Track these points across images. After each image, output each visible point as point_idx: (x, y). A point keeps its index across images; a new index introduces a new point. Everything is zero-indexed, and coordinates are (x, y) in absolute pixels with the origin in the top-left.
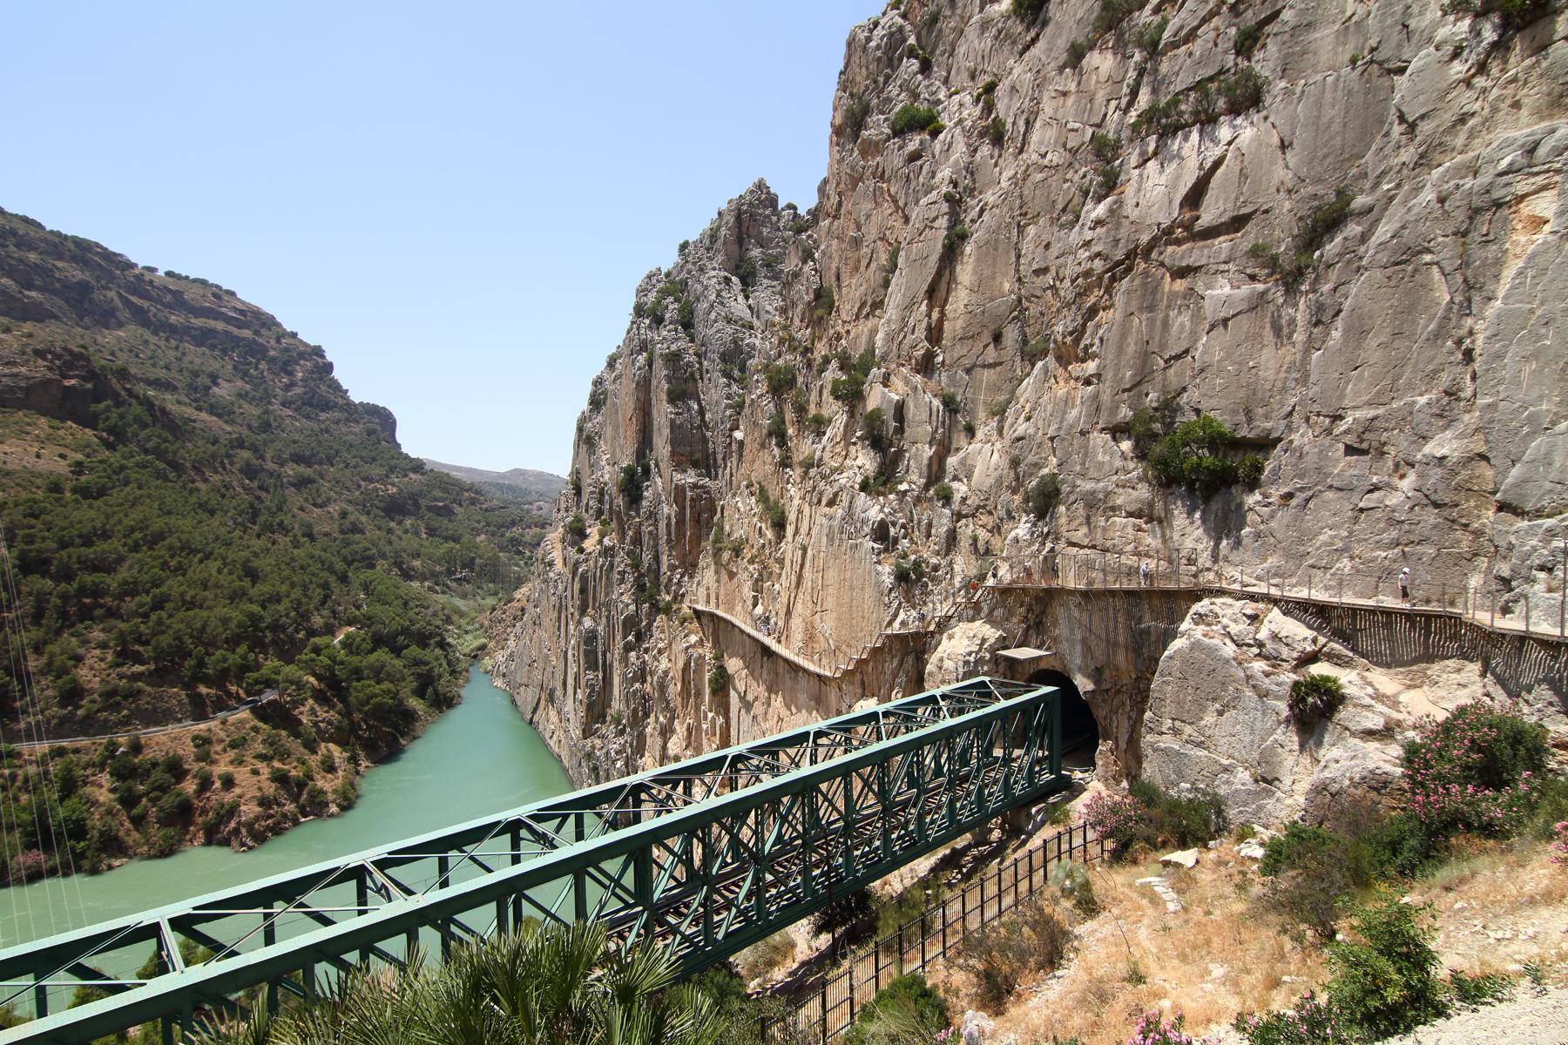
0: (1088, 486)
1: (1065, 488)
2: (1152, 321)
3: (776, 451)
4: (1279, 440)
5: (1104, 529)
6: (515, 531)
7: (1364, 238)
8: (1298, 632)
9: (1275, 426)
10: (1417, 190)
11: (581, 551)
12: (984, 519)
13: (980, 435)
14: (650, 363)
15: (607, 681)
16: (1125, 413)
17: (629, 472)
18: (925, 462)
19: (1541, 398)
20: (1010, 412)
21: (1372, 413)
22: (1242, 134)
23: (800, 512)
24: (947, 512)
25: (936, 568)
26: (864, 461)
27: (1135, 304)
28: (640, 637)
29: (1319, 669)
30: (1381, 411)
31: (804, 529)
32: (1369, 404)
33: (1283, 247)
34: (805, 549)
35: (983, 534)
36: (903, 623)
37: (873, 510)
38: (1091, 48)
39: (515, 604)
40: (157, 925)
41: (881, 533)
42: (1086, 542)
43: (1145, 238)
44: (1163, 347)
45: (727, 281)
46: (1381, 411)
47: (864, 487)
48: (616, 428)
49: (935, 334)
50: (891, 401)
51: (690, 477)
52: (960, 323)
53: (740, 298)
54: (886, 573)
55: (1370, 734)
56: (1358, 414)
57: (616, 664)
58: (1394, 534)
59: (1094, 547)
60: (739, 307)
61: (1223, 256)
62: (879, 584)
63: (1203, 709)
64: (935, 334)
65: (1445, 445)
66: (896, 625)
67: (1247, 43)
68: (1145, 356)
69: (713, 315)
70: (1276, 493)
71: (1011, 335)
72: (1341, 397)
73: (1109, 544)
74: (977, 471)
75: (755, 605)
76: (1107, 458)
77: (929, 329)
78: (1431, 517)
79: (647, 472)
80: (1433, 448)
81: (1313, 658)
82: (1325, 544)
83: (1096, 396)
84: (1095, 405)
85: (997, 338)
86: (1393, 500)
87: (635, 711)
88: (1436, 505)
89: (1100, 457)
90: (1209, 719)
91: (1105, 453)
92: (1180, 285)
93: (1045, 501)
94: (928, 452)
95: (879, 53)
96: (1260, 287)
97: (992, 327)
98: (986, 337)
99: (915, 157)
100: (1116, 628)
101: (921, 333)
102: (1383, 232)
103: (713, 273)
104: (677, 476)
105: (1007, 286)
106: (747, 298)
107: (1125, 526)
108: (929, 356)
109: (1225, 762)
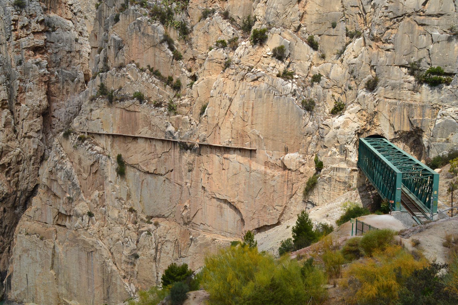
5: (399, 94)
12: (337, 90)
13: (327, 59)
16: (405, 62)
42: (392, 97)
47: (278, 76)
49: (302, 17)
59: (395, 99)
61: (436, 24)
64: (302, 17)
71: (341, 27)
73: (401, 98)
76: (399, 74)
85: (334, 26)
90: (450, 136)
91: (397, 72)
96: (449, 35)
97: (331, 21)
100: (404, 121)
107: (408, 93)
109: (455, 144)
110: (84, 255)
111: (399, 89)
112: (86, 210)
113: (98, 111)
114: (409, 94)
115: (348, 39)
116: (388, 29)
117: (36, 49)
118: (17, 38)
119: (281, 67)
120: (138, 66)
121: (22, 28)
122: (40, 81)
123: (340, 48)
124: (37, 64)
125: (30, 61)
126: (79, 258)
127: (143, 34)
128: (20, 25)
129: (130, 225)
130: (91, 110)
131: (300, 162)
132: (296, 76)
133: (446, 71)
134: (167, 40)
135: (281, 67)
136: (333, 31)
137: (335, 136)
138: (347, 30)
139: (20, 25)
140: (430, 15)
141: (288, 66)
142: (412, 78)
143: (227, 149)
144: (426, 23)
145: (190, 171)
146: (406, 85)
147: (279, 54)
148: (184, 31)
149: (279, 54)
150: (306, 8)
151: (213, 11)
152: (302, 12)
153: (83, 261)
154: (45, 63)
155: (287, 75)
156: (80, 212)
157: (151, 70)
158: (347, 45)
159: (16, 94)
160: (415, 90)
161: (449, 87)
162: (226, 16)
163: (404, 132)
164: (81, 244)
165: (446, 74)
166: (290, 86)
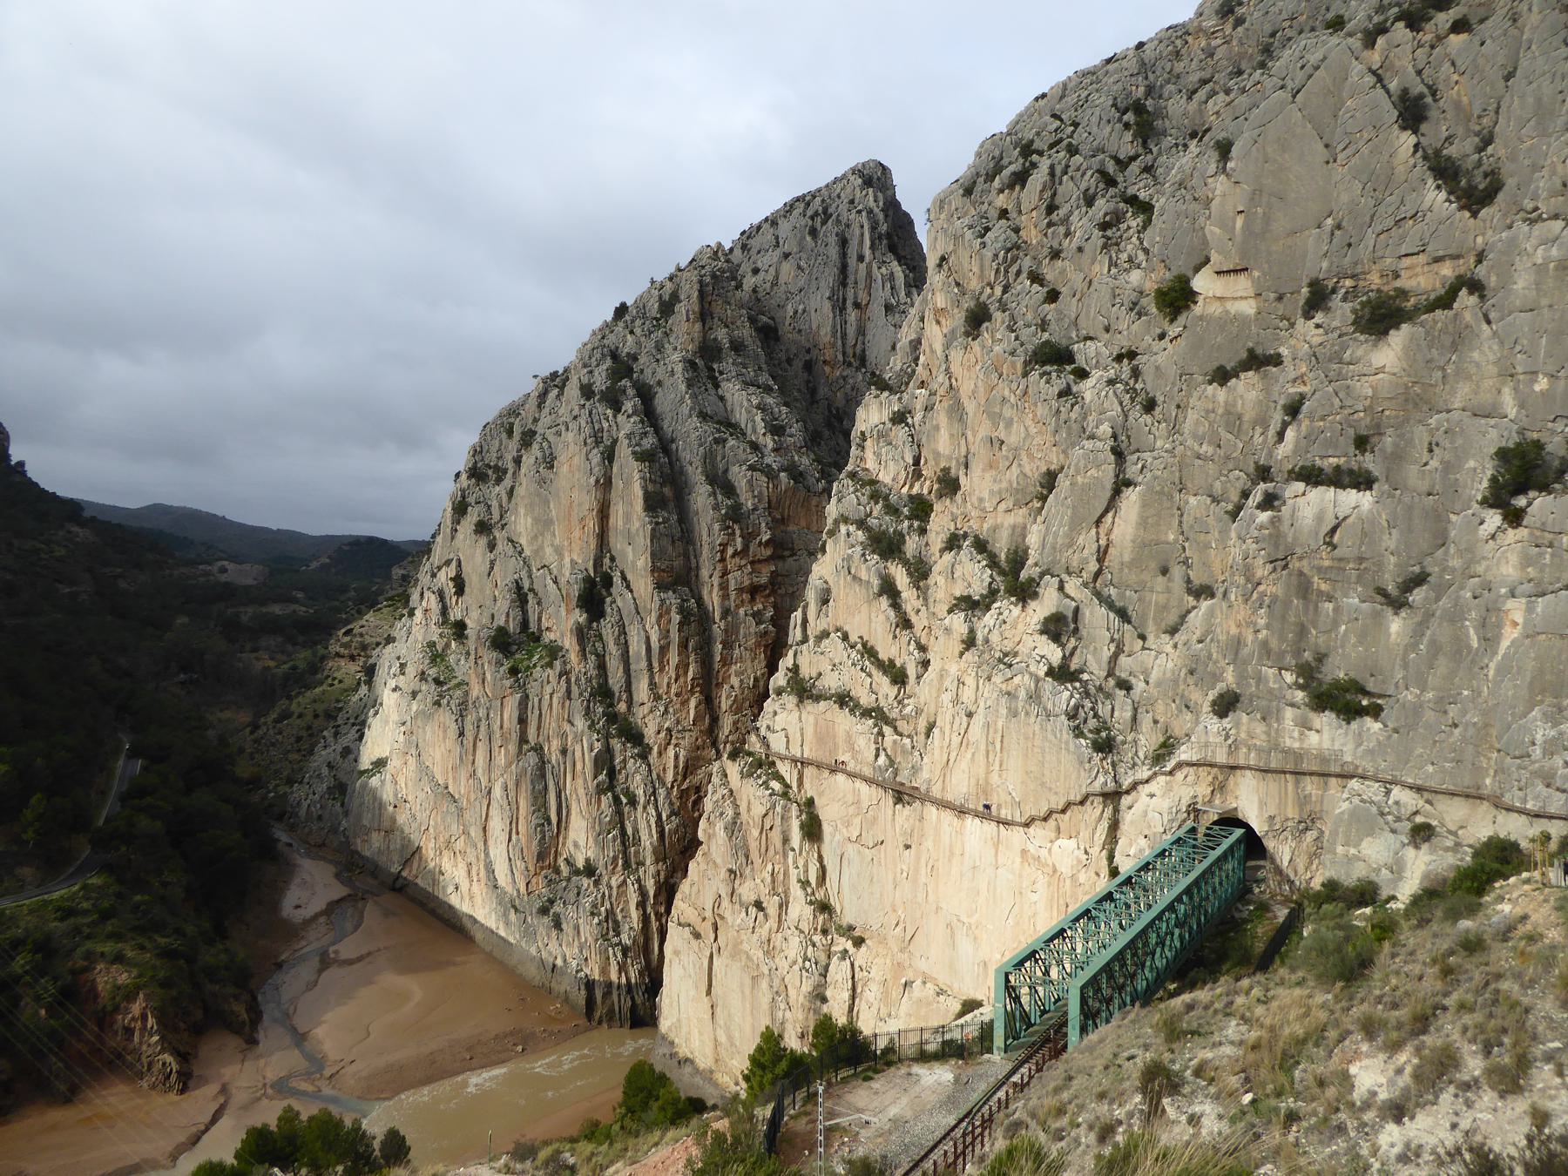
13: (1151, 642)
17: (589, 583)
23: (961, 682)
29: (1419, 819)
33: (1391, 588)
34: (970, 715)
48: (544, 525)
55: (1447, 849)
71: (1177, 572)
75: (877, 756)
79: (608, 581)
81: (1416, 813)
85: (1165, 571)
87: (615, 859)
90: (1365, 844)
93: (1226, 705)
94: (1107, 652)
102: (1444, 602)
105: (1171, 537)
110: (748, 982)
112: (753, 898)
113: (785, 714)
114: (1296, 734)
115: (1191, 600)
117: (754, 591)
118: (725, 573)
119: (1055, 654)
120: (845, 637)
121: (733, 556)
122: (758, 645)
123: (1172, 618)
124: (754, 615)
125: (742, 611)
126: (742, 985)
127: (855, 578)
128: (730, 551)
129: (816, 938)
130: (775, 713)
131: (1079, 861)
132: (1085, 677)
134: (889, 589)
135: (1055, 654)
137: (1145, 813)
138: (1189, 581)
139: (730, 551)
141: (1072, 654)
142: (1300, 695)
143: (962, 811)
145: (908, 847)
146: (1289, 713)
147: (1056, 627)
148: (920, 572)
149: (1056, 627)
150: (1112, 537)
151: (965, 536)
152: (1103, 542)
153: (747, 991)
154: (769, 613)
155: (1063, 674)
156: (744, 898)
157: (864, 645)
158: (1189, 612)
159: (716, 666)
160: (1305, 725)
162: (981, 546)
164: (744, 958)
166: (1063, 697)
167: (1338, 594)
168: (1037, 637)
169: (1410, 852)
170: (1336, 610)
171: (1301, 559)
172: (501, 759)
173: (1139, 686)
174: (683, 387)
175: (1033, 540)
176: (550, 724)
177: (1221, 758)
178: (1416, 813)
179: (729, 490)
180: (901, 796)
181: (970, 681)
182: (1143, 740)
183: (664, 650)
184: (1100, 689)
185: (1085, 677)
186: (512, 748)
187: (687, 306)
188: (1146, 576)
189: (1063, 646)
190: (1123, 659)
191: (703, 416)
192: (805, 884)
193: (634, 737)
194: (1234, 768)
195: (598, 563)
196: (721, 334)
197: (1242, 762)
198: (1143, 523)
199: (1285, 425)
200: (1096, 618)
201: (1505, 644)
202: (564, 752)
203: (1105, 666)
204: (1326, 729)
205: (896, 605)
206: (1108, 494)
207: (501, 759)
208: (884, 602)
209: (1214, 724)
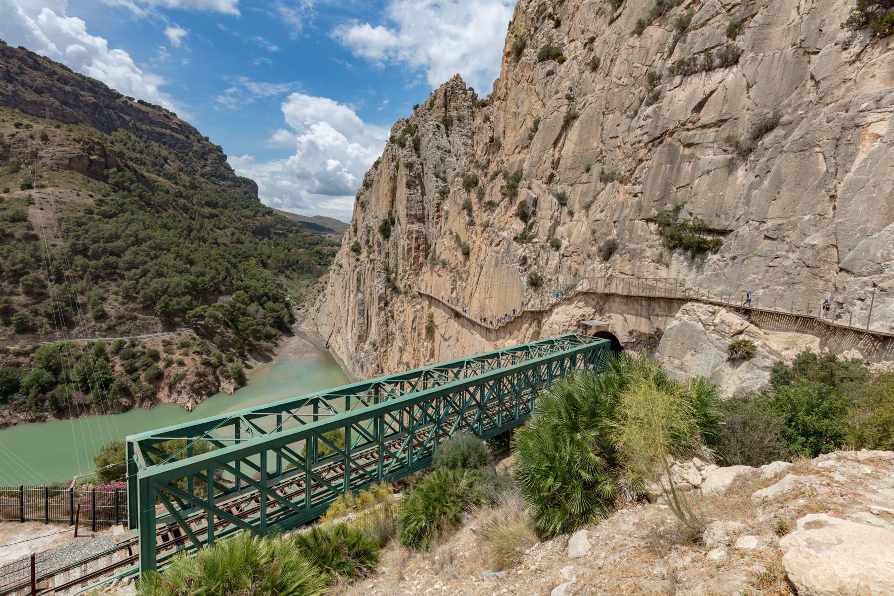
0: (633, 246)
1: (620, 246)
2: (672, 169)
3: (467, 218)
4: (732, 231)
5: (639, 267)
6: (318, 247)
7: (785, 137)
8: (736, 321)
9: (733, 225)
10: (816, 116)
11: (358, 260)
12: (575, 258)
13: (576, 217)
14: (397, 167)
15: (368, 325)
16: (654, 212)
17: (386, 223)
18: (547, 228)
19: (867, 221)
20: (593, 207)
21: (780, 222)
22: (730, 76)
23: (480, 249)
24: (557, 253)
25: (550, 280)
26: (518, 226)
27: (663, 160)
28: (386, 304)
30: (785, 221)
31: (482, 256)
32: (779, 217)
34: (481, 267)
35: (574, 266)
36: (533, 306)
37: (520, 250)
38: (650, 24)
39: (319, 284)
40: (239, 418)
41: (524, 261)
42: (629, 272)
43: (671, 127)
44: (677, 180)
45: (438, 127)
46: (785, 221)
47: (515, 239)
48: (378, 199)
49: (556, 164)
50: (531, 197)
51: (415, 227)
52: (569, 161)
53: (445, 136)
54: (525, 279)
56: (773, 221)
57: (374, 317)
58: (786, 278)
60: (444, 142)
61: (711, 139)
62: (522, 286)
63: (685, 353)
64: (556, 164)
65: (816, 239)
66: (530, 305)
67: (733, 31)
68: (667, 185)
69: (431, 144)
70: (728, 255)
71: (596, 168)
72: (766, 212)
74: (574, 235)
75: (452, 292)
77: (553, 162)
78: (805, 272)
79: (393, 223)
80: (809, 240)
81: (741, 332)
82: (751, 281)
83: (639, 203)
84: (640, 208)
85: (588, 170)
86: (787, 263)
87: (383, 340)
88: (808, 267)
89: (639, 233)
90: (688, 357)
91: (642, 230)
92: (687, 151)
93: (609, 251)
94: (548, 224)
95: (532, 15)
96: (730, 156)
97: (586, 164)
98: (583, 169)
99: (550, 73)
101: (548, 164)
102: (796, 134)
103: (432, 123)
104: (409, 226)
105: (595, 144)
106: (448, 136)
108: (552, 176)
111: (640, 259)
114: (652, 269)
115: (602, 185)
116: (641, 161)
120: (451, 233)
123: (589, 199)
133: (714, 226)
136: (585, 178)
138: (603, 173)
140: (704, 127)
141: (531, 227)
144: (695, 141)
152: (556, 156)
161: (716, 257)
163: (641, 334)
165: (711, 232)
167: (698, 154)
168: (514, 218)
169: (727, 369)
170: (695, 168)
171: (672, 134)
172: (352, 295)
173: (565, 243)
174: (431, 135)
175: (526, 166)
176: (368, 283)
177: (601, 289)
178: (741, 332)
179: (444, 180)
180: (457, 315)
181: (483, 247)
182: (561, 279)
183: (409, 250)
184: (542, 247)
185: (535, 240)
186: (355, 292)
187: (439, 102)
188: (578, 173)
189: (526, 222)
190: (560, 229)
191: (438, 148)
192: (424, 357)
193: (396, 290)
194: (608, 296)
195: (390, 213)
196: (454, 113)
197: (613, 291)
198: (581, 141)
199: (676, 40)
200: (548, 204)
201: (861, 157)
202: (371, 294)
203: (547, 233)
204: (674, 263)
205: (470, 214)
206: (562, 123)
207: (352, 295)
208: (465, 212)
209: (597, 264)
